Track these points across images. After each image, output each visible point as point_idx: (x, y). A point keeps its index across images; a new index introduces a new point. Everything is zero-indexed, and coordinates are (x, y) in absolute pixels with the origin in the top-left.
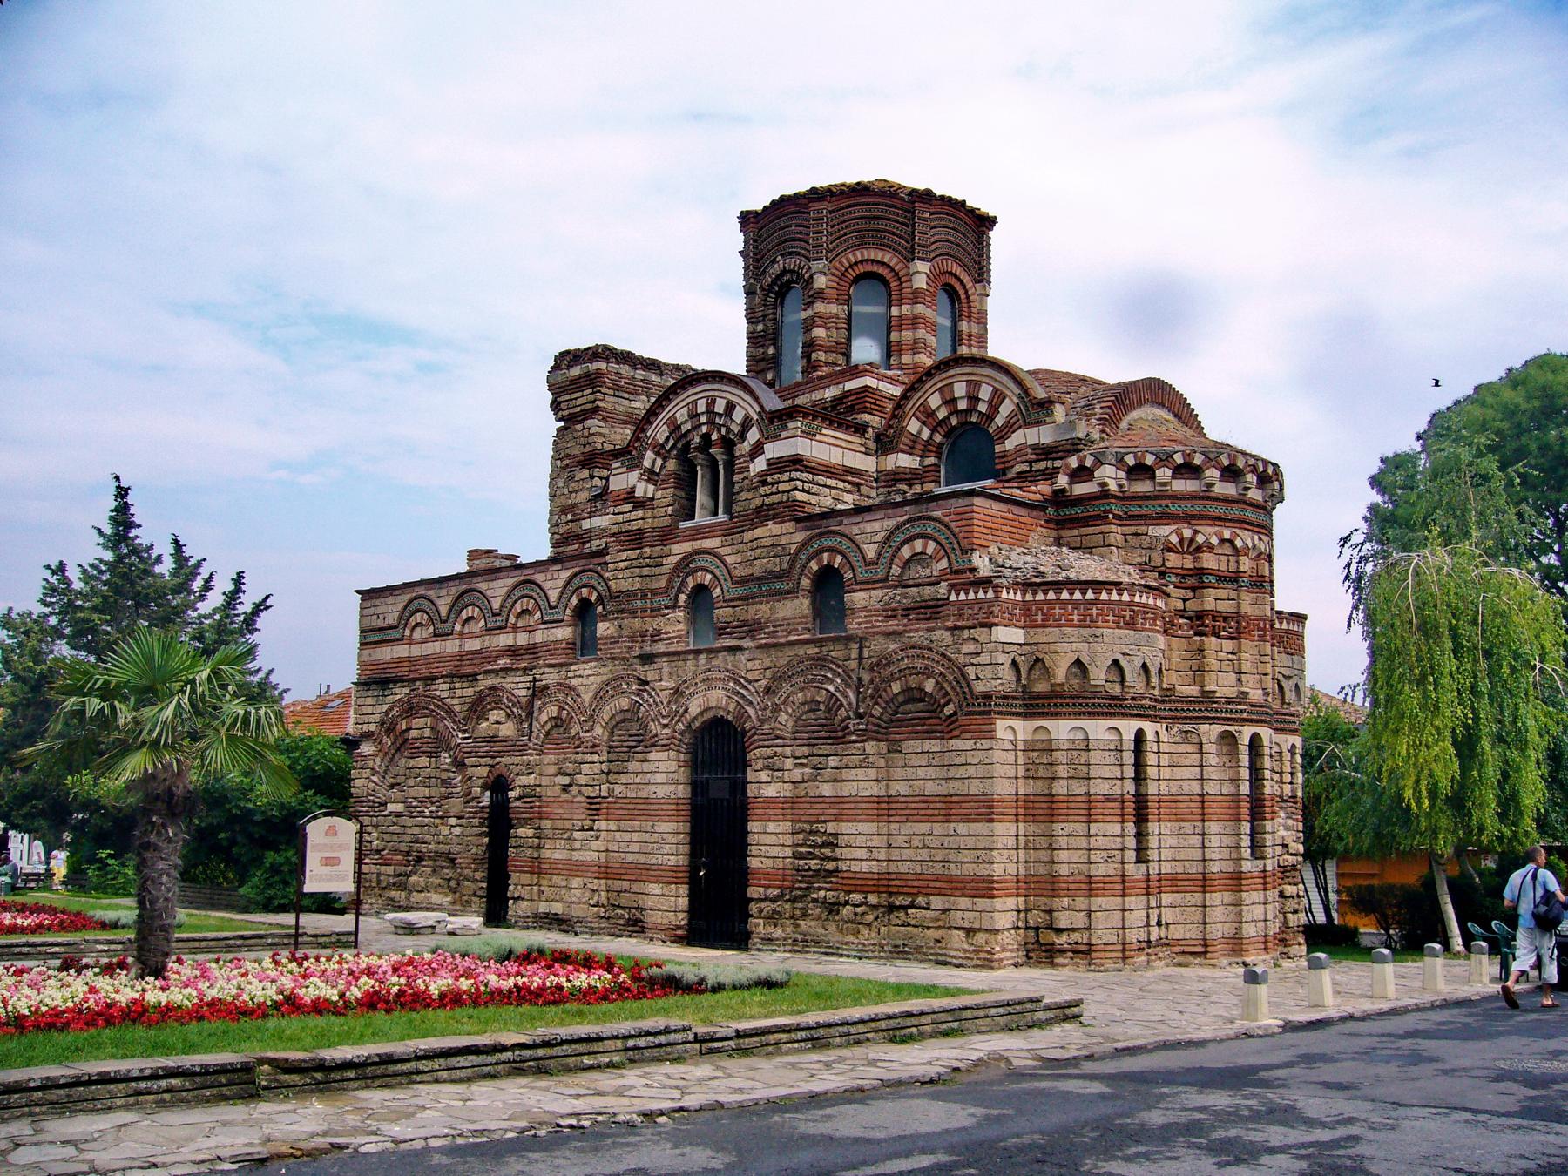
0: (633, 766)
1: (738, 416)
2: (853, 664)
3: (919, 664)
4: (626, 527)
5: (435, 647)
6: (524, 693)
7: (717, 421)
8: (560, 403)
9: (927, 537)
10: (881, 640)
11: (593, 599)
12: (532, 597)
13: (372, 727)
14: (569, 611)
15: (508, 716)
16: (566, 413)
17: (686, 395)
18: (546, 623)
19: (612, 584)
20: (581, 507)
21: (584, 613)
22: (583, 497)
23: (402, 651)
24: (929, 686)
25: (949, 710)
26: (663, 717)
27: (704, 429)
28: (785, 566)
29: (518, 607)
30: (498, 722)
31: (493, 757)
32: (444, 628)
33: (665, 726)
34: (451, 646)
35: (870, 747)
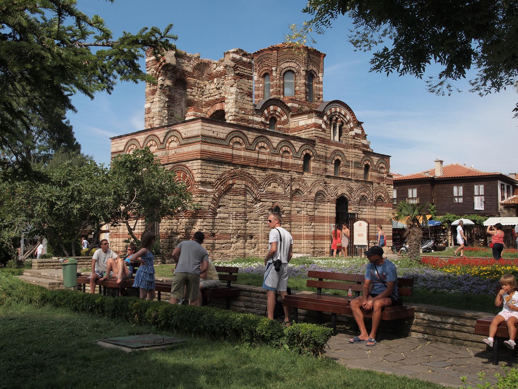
0: (320, 207)
1: (348, 117)
2: (371, 188)
3: (382, 191)
4: (320, 136)
5: (248, 154)
6: (286, 179)
7: (341, 116)
8: (238, 67)
9: (383, 163)
10: (376, 184)
11: (311, 154)
12: (289, 147)
13: (213, 180)
14: (302, 156)
15: (279, 185)
16: (241, 72)
17: (334, 104)
18: (295, 157)
19: (318, 153)
20: (248, 110)
21: (307, 158)
22: (249, 107)
23: (229, 151)
24: (383, 195)
25: (386, 201)
26: (332, 194)
27: (337, 116)
28: (360, 161)
29: (284, 148)
30: (275, 187)
31: (273, 199)
32: (251, 148)
33: (332, 196)
34: (254, 155)
35: (374, 207)
